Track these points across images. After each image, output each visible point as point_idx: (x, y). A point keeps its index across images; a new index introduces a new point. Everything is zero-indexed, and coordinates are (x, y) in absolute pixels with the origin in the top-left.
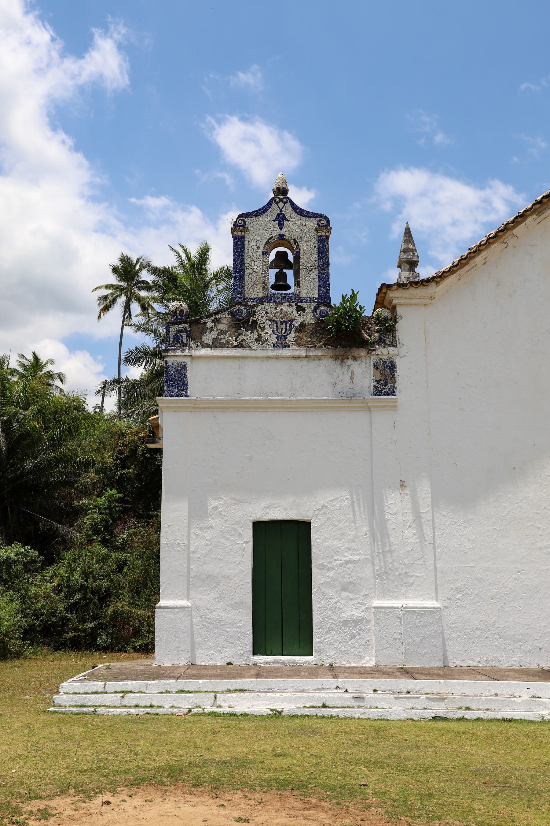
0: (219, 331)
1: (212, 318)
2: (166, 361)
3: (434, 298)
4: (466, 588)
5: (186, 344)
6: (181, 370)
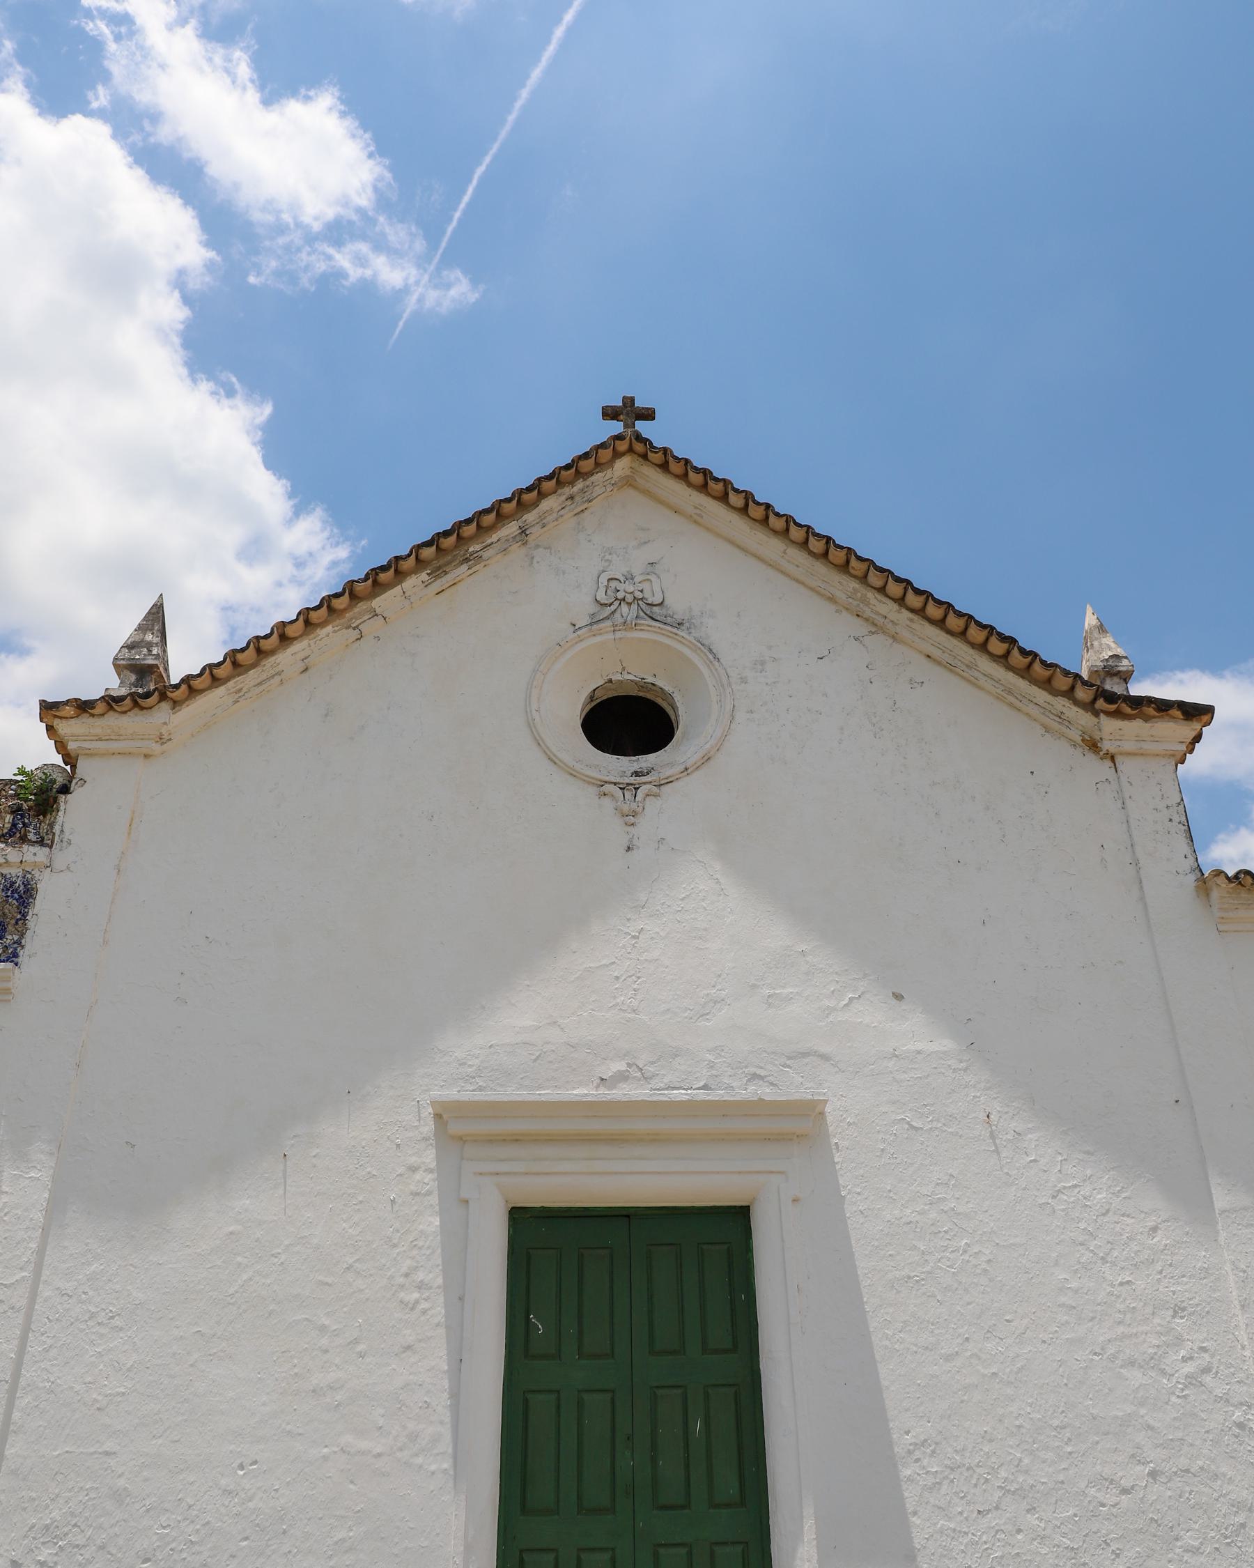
3: (170, 739)
4: (75, 1525)
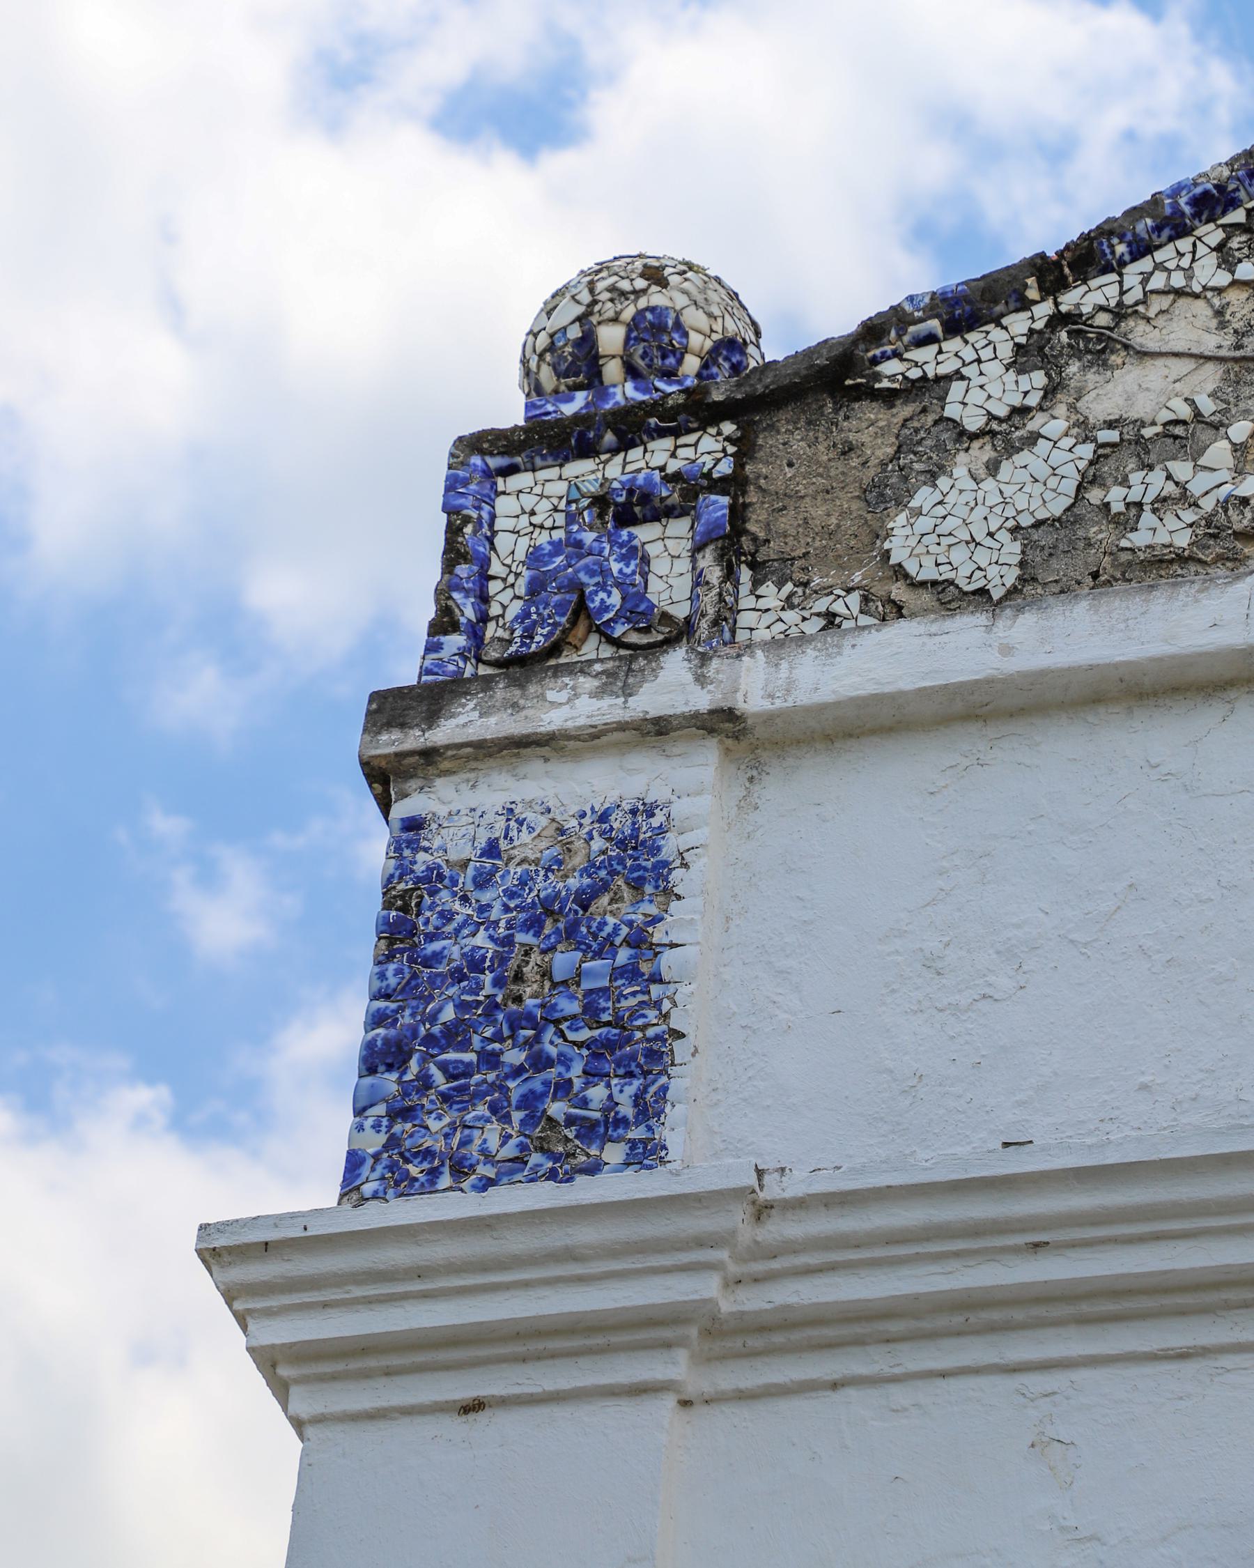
0: (1112, 436)
1: (1019, 324)
2: (414, 825)
5: (681, 632)
6: (585, 900)
